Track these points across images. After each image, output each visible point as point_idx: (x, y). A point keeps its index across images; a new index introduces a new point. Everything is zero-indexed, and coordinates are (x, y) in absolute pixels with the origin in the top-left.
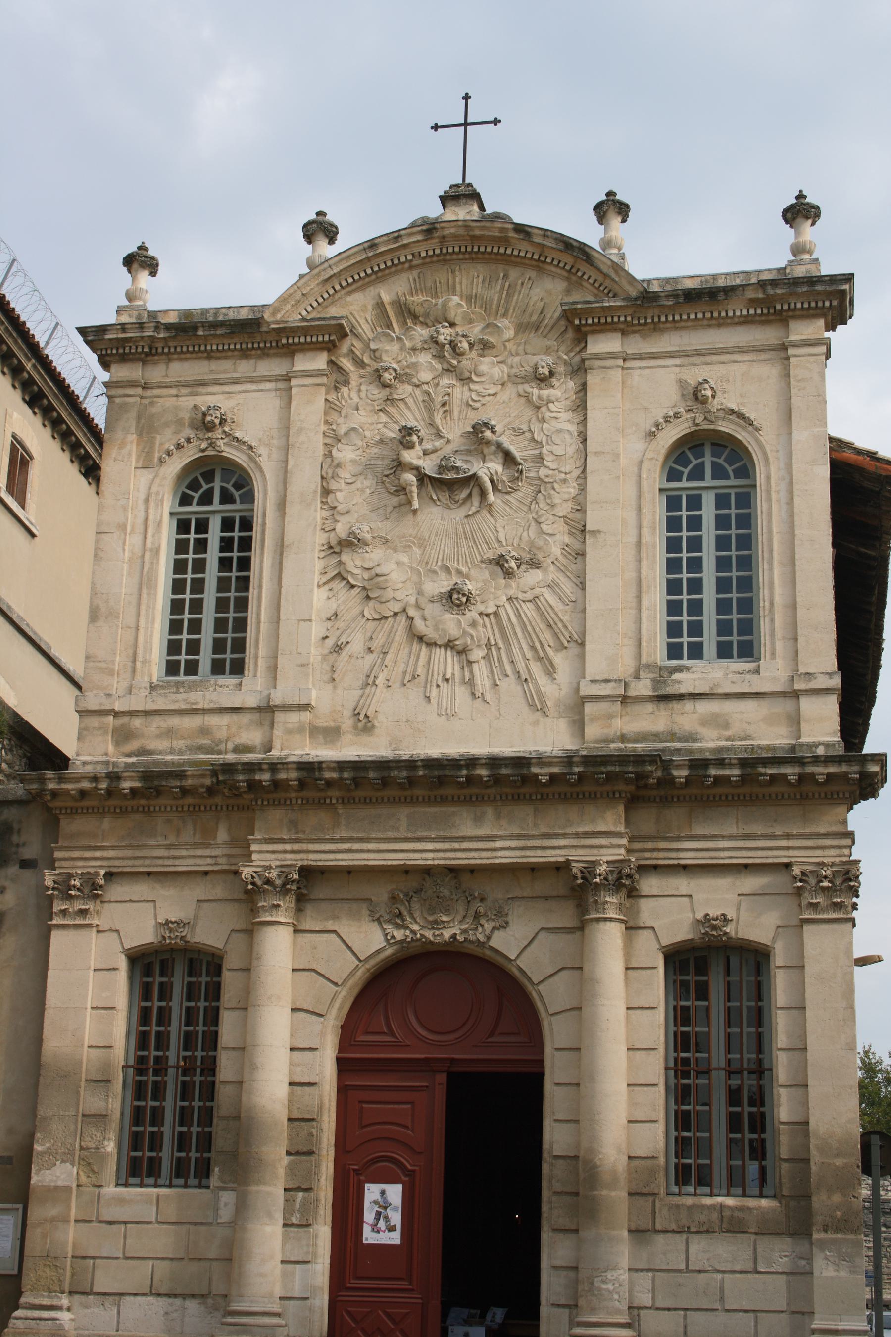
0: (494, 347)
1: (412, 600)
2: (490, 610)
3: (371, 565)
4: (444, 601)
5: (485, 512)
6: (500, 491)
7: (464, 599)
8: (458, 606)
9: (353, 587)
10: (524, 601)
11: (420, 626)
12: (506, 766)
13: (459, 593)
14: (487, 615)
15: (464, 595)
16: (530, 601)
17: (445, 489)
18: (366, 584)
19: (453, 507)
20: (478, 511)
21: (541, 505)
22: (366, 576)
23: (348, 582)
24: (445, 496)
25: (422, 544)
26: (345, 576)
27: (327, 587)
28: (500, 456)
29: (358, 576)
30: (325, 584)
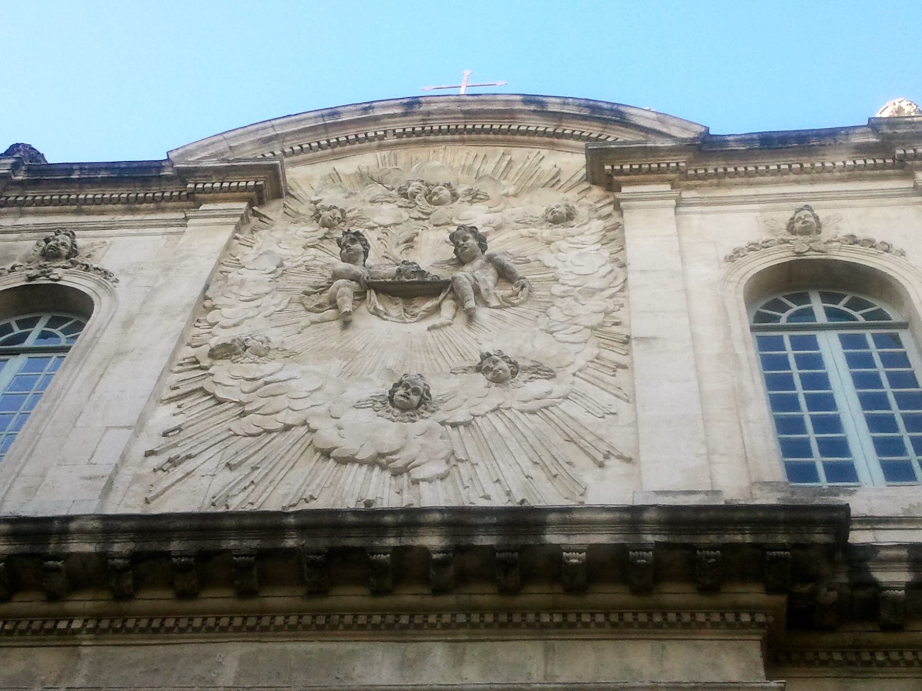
0: (487, 198)
1: (322, 410)
2: (460, 419)
3: (258, 375)
4: (379, 405)
5: (460, 321)
6: (487, 304)
7: (415, 399)
8: (404, 408)
9: (220, 402)
10: (522, 412)
11: (328, 434)
12: (487, 529)
13: (407, 386)
14: (454, 425)
15: (416, 391)
16: (533, 412)
17: (400, 300)
18: (244, 398)
19: (408, 320)
20: (450, 324)
21: (553, 317)
22: (247, 386)
23: (214, 397)
24: (395, 310)
25: (350, 356)
26: (209, 387)
27: (174, 405)
28: (492, 270)
29: (231, 390)
30: (171, 400)
